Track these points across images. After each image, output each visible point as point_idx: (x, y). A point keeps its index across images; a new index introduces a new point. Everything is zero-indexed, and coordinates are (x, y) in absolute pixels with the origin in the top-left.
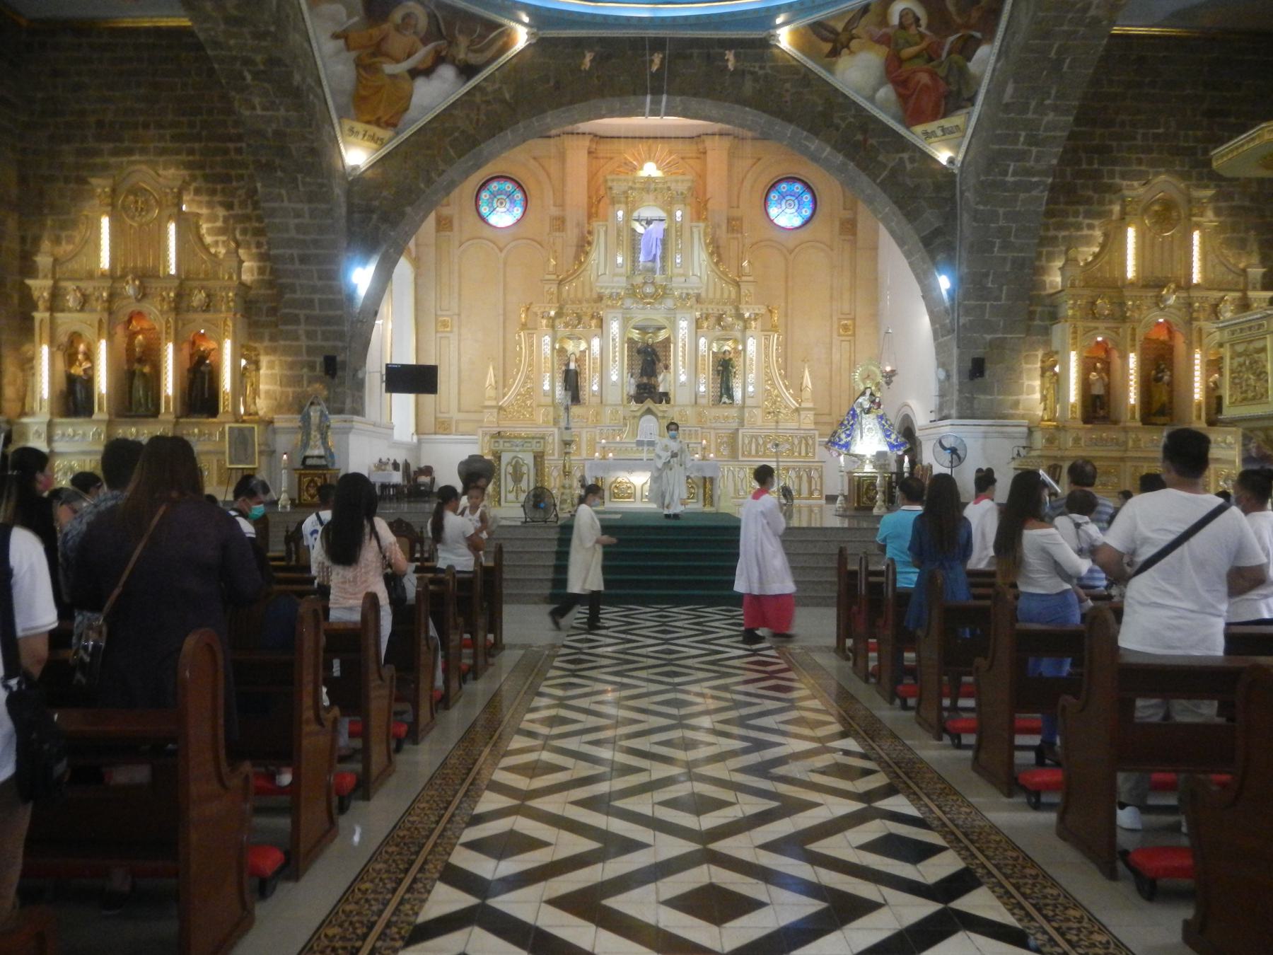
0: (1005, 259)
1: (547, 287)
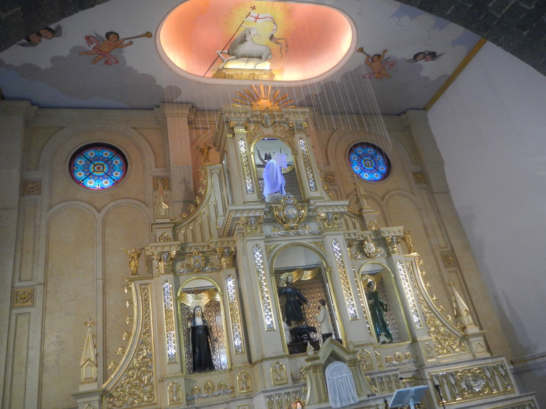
1: (159, 233)
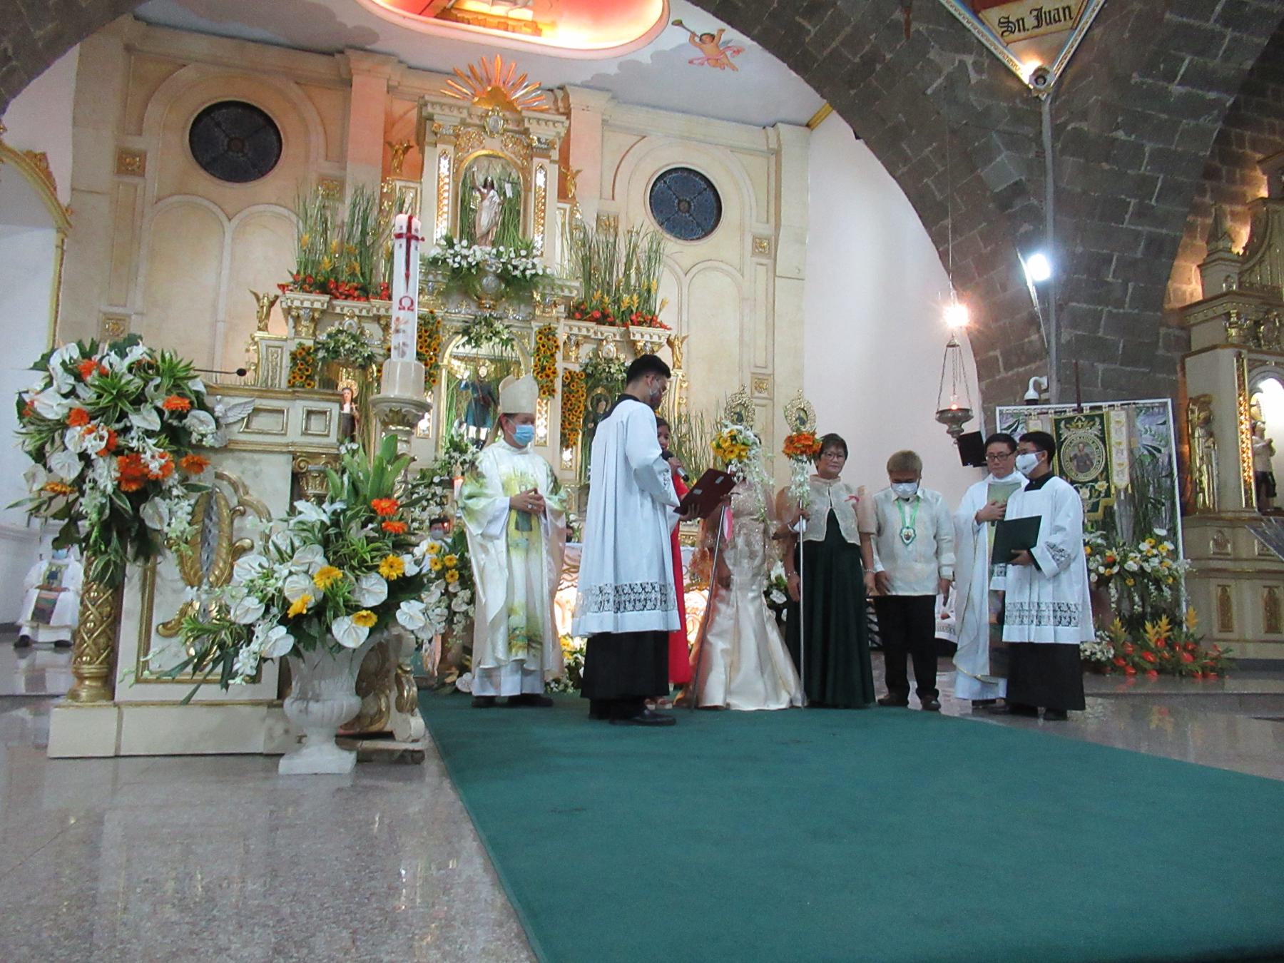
0: (1138, 235)
